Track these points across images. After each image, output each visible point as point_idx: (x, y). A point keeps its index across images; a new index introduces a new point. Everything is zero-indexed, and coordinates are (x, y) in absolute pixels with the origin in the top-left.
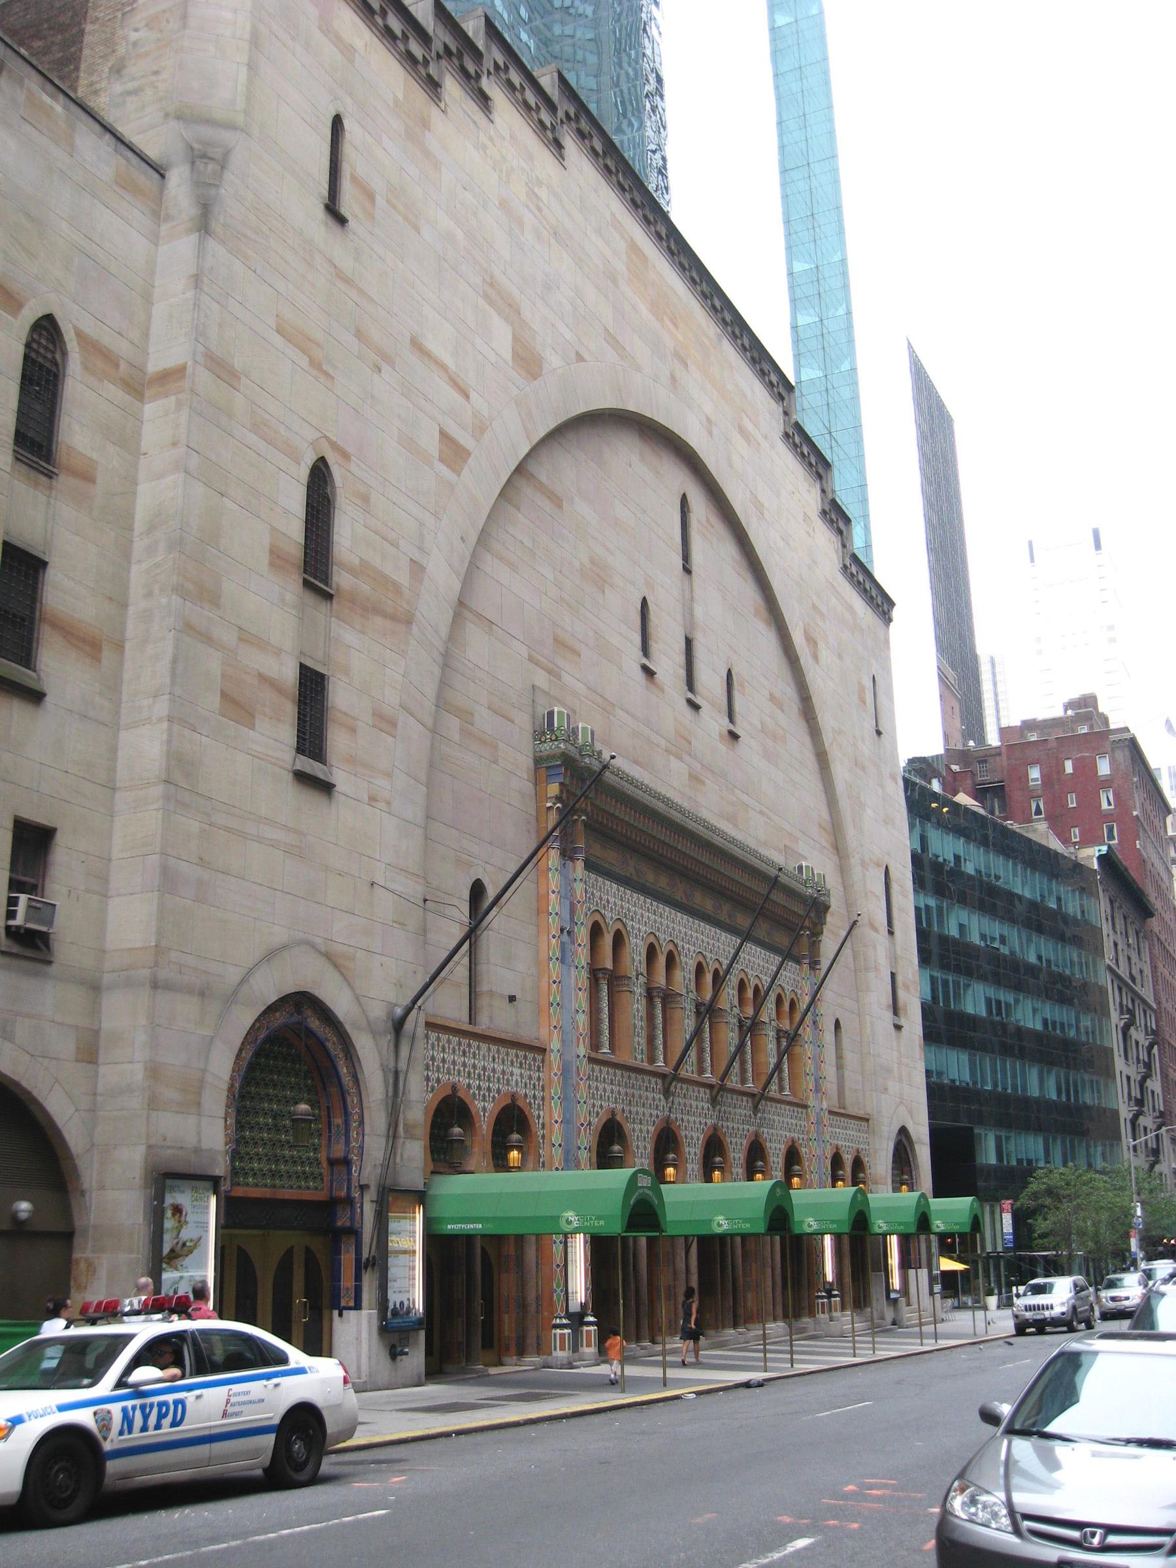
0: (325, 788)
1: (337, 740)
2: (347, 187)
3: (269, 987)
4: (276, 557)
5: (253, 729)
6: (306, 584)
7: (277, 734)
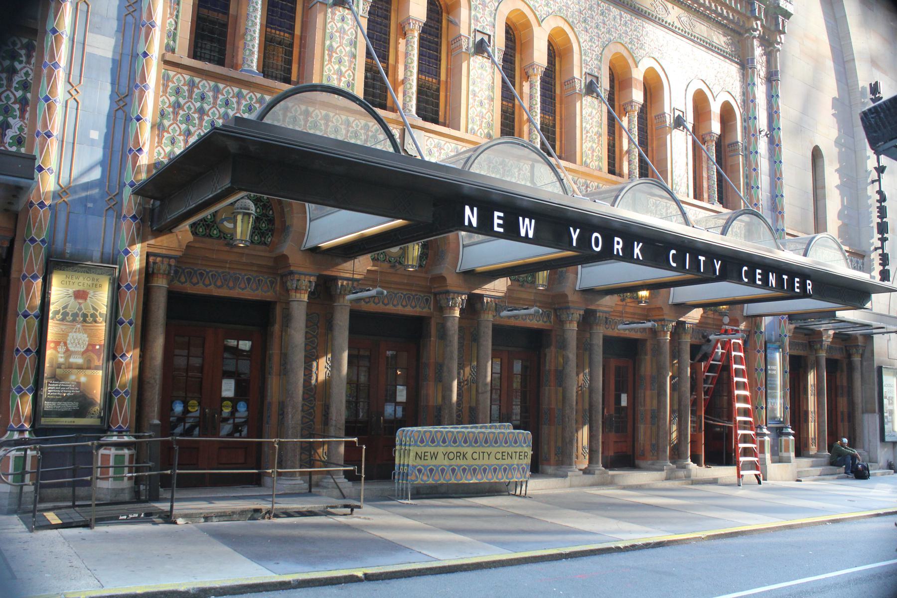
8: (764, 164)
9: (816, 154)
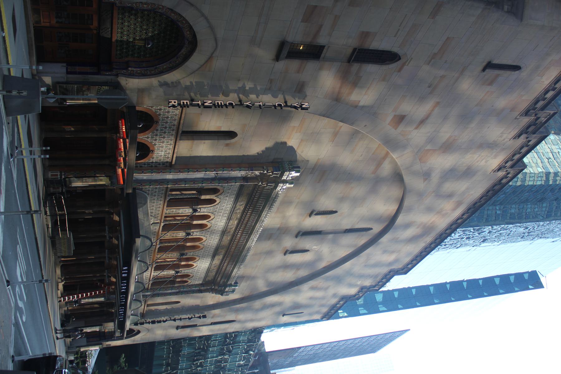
0: (277, 58)
1: (294, 64)
2: (497, 72)
3: (200, 28)
4: (365, 35)
5: (302, 21)
6: (355, 50)
7: (298, 35)
8: (170, 291)
9: (178, 302)
